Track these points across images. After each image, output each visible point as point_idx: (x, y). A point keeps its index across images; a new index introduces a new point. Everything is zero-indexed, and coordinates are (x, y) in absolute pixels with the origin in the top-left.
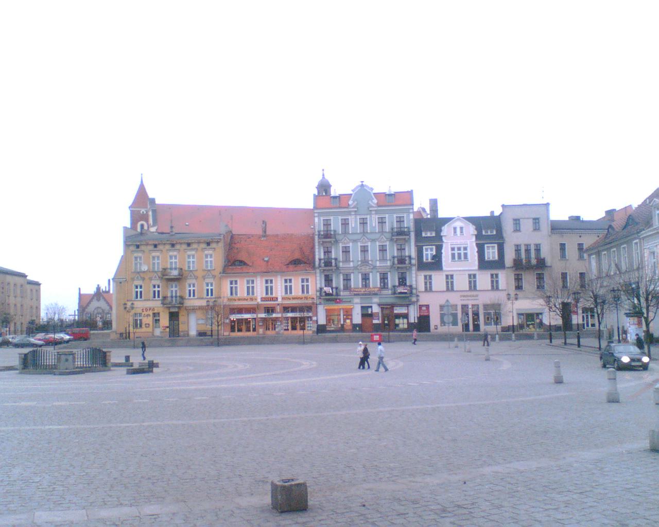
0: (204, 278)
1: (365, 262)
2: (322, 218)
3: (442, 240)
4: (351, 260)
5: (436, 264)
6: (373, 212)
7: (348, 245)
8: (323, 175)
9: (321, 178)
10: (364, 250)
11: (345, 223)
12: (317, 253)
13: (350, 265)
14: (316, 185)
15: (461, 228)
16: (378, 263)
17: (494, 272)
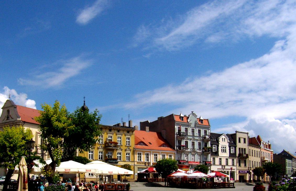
0: (126, 150)
3: (219, 143)
5: (216, 154)
6: (197, 127)
10: (193, 144)
11: (186, 130)
12: (176, 143)
13: (188, 150)
15: (224, 139)
16: (198, 150)
17: (233, 158)
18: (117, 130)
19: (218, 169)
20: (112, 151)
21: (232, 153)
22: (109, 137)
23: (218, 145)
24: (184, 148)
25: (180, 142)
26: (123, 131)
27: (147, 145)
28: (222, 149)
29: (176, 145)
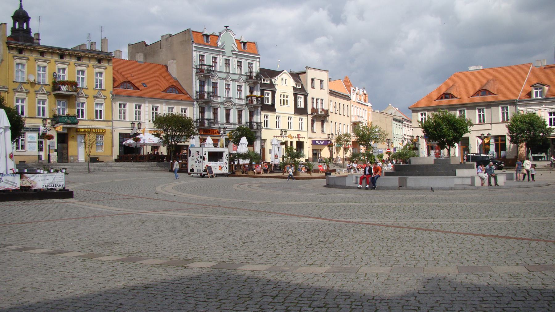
0: (95, 97)
1: (228, 100)
2: (198, 53)
3: (275, 88)
4: (219, 95)
5: (271, 108)
7: (216, 82)
8: (21, 6)
9: (18, 8)
12: (194, 86)
14: (12, 14)
18: (75, 56)
19: (274, 136)
20: (65, 100)
21: (299, 107)
22: (59, 69)
23: (275, 91)
24: (211, 96)
25: (203, 84)
26: (90, 58)
27: (139, 89)
28: (281, 99)
29: (194, 89)
